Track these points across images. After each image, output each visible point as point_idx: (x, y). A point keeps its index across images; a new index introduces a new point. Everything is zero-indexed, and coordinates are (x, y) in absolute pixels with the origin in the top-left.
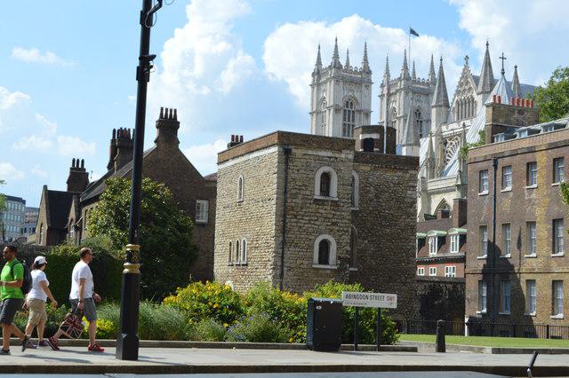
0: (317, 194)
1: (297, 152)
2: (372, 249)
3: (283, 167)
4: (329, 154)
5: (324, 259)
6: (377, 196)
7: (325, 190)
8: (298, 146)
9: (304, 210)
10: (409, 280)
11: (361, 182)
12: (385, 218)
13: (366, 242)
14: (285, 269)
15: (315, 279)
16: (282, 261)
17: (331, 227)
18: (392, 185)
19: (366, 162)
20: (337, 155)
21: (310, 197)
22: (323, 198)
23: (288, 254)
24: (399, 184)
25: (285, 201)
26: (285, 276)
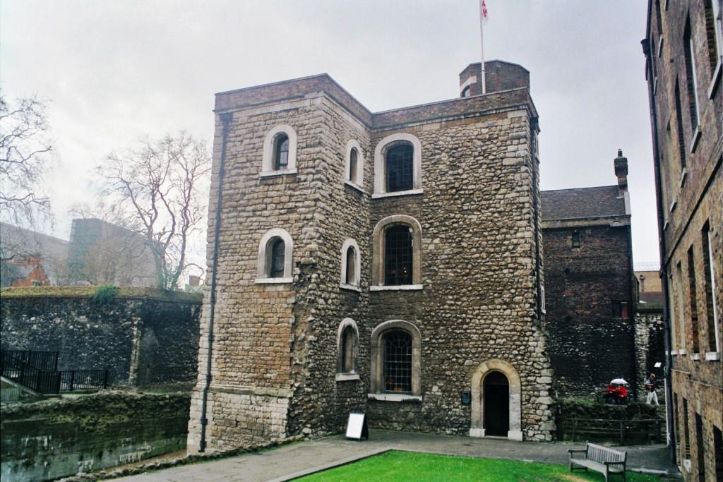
0: (267, 170)
1: (241, 116)
2: (447, 251)
3: (221, 141)
4: (287, 106)
5: (275, 271)
6: (453, 166)
7: (277, 164)
8: (241, 108)
9: (246, 197)
10: (517, 299)
11: (425, 149)
12: (469, 199)
13: (437, 241)
14: (218, 288)
15: (261, 301)
16: (214, 279)
17: (285, 217)
18: (479, 143)
19: (431, 120)
20: (296, 105)
21: (256, 177)
22: (274, 173)
23: (222, 266)
24: (489, 140)
25: (221, 189)
26: (218, 301)
